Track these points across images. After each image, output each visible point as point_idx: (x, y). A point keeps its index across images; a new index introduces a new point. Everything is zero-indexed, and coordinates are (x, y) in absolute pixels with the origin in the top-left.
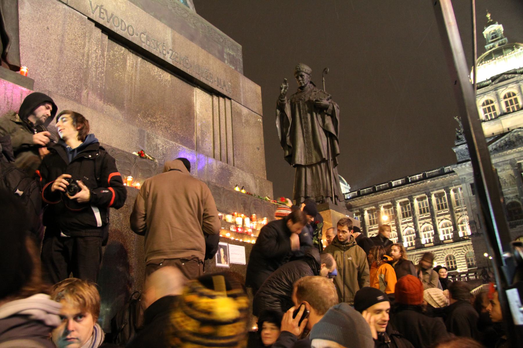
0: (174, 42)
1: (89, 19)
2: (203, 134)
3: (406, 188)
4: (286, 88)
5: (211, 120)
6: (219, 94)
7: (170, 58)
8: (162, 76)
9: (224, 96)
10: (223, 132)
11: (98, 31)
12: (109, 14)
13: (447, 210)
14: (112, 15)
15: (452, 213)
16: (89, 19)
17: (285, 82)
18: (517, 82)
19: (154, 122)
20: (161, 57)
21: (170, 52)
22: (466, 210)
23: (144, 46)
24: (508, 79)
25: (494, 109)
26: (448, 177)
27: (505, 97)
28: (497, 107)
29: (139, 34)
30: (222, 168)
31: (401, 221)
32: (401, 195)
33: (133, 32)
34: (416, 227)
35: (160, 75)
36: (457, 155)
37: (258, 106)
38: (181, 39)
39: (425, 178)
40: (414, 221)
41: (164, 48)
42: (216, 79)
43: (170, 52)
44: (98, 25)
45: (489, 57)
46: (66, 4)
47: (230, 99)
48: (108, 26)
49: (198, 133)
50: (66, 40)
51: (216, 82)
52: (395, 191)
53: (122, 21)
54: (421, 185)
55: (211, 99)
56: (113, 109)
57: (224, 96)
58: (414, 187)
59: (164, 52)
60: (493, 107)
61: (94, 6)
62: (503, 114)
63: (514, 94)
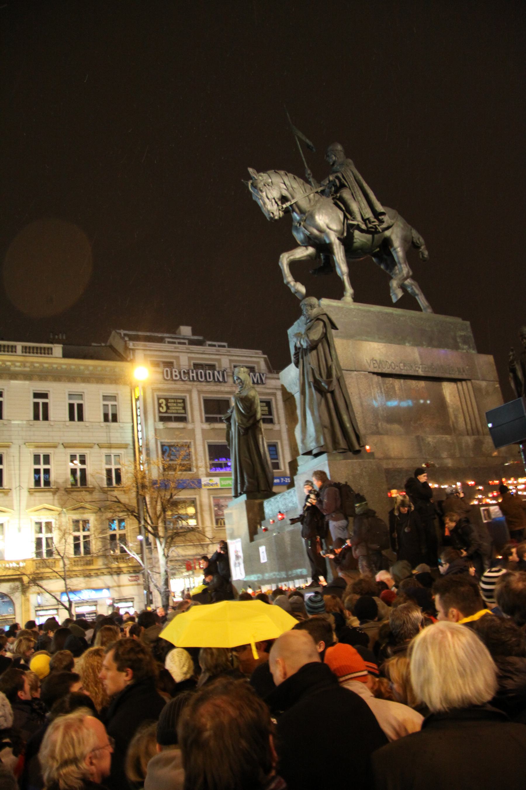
0: (421, 357)
1: (369, 372)
2: (456, 417)
4: (513, 355)
5: (459, 403)
6: (461, 380)
7: (422, 371)
8: (419, 386)
9: (465, 380)
10: (470, 409)
11: (375, 376)
12: (378, 361)
14: (380, 361)
16: (369, 372)
17: (512, 350)
19: (422, 424)
20: (416, 374)
21: (421, 366)
23: (404, 372)
29: (398, 365)
30: (476, 441)
33: (395, 366)
35: (417, 386)
37: (493, 374)
38: (426, 350)
41: (416, 366)
42: (456, 370)
43: (421, 366)
44: (374, 373)
46: (355, 371)
47: (470, 380)
48: (380, 371)
49: (452, 417)
50: (362, 395)
51: (457, 372)
53: (387, 362)
55: (455, 386)
56: (396, 427)
57: (465, 380)
59: (417, 369)
61: (369, 361)
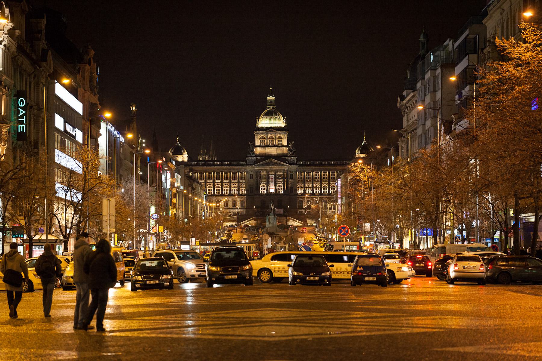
3: (221, 167)
13: (237, 181)
15: (239, 182)
18: (275, 134)
22: (245, 182)
24: (273, 131)
25: (264, 142)
26: (240, 167)
27: (269, 138)
28: (266, 141)
31: (216, 181)
32: (218, 170)
34: (222, 186)
36: (247, 161)
39: (230, 165)
40: (222, 182)
45: (267, 115)
52: (216, 167)
54: (228, 167)
58: (224, 168)
60: (264, 140)
62: (268, 146)
63: (273, 138)
